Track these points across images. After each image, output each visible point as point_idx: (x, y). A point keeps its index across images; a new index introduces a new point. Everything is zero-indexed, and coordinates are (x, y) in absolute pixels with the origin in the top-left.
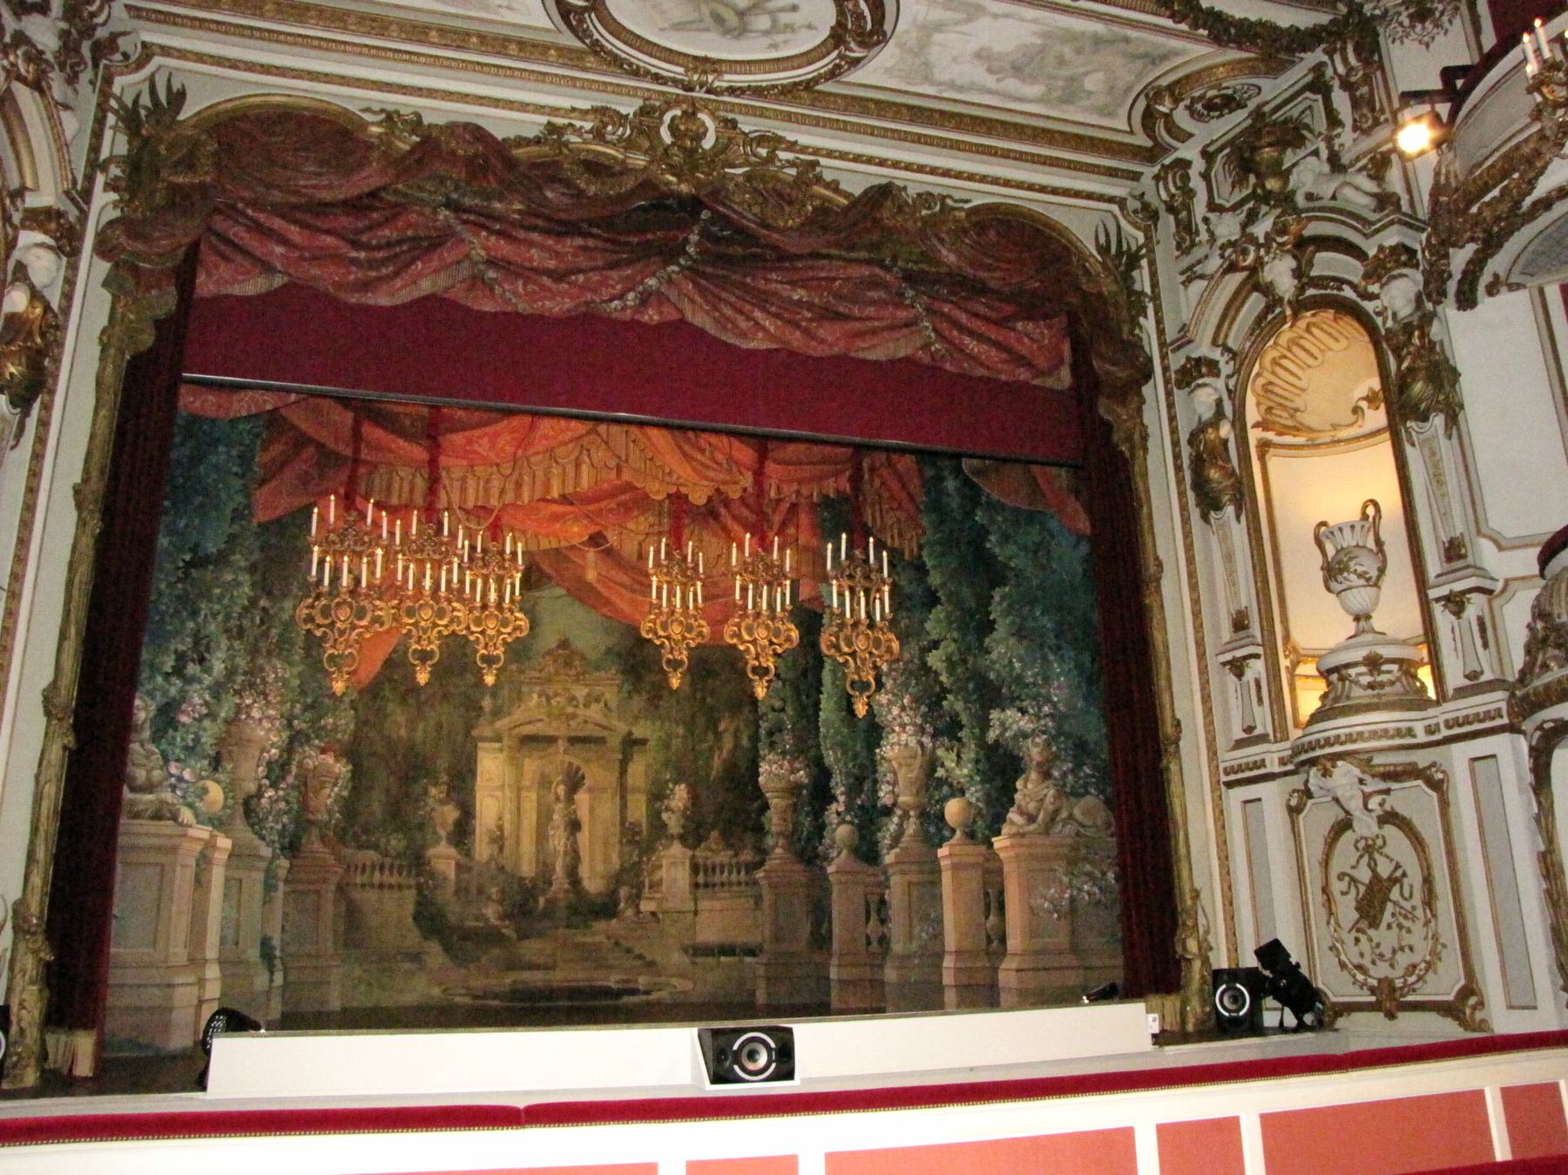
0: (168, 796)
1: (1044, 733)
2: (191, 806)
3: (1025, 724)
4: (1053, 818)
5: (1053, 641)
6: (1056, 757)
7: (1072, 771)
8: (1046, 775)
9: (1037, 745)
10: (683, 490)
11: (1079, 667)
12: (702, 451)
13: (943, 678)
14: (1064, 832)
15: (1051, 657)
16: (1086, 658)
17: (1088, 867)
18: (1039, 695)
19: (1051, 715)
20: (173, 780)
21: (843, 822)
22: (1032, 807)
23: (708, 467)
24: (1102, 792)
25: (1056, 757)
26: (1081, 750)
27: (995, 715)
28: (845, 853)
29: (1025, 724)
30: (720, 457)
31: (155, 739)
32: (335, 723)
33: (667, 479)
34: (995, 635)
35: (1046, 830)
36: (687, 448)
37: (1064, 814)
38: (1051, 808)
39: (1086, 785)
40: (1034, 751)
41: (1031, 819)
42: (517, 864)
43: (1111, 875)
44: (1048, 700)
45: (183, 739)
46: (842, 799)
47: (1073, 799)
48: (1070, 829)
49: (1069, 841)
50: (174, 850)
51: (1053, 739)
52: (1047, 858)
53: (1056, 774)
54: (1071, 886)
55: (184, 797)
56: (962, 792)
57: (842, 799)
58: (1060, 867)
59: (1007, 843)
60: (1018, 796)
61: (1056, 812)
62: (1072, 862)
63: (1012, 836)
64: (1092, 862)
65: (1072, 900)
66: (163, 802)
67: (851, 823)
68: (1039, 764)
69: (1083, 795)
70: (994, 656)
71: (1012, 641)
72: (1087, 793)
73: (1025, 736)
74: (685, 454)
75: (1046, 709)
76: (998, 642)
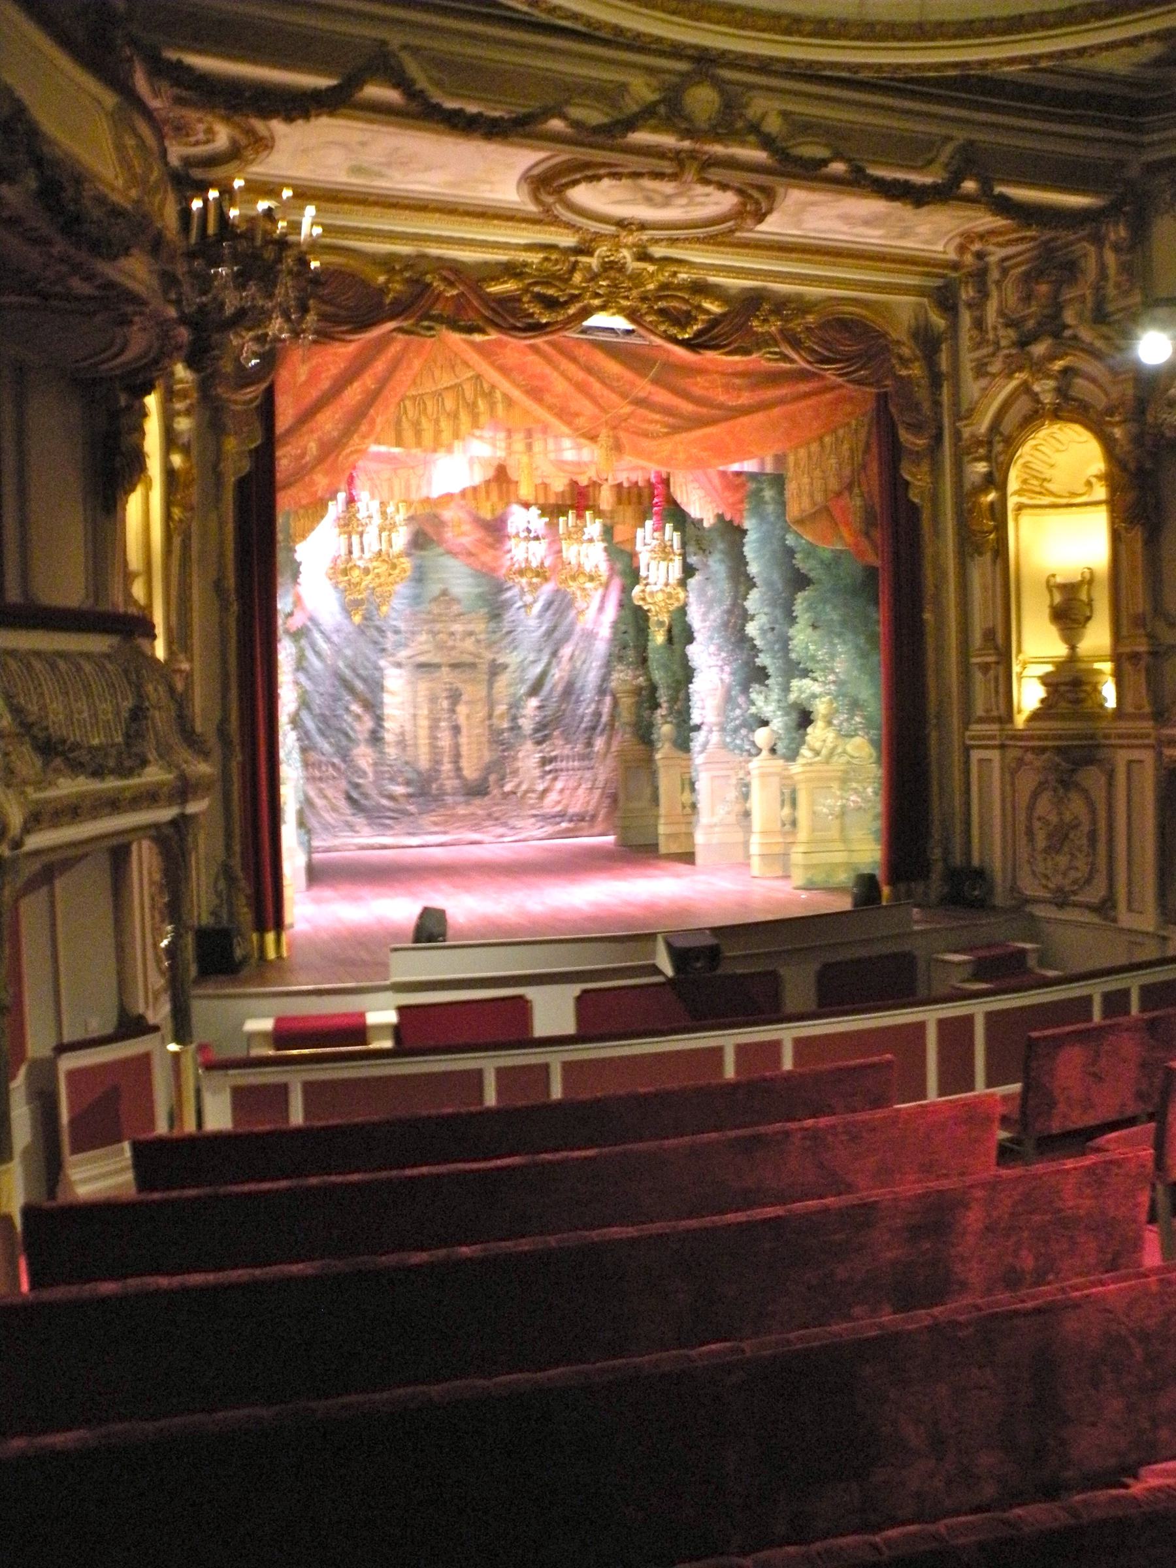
1: (828, 694)
3: (816, 688)
4: (832, 753)
5: (838, 630)
6: (837, 711)
7: (847, 720)
8: (829, 723)
9: (823, 703)
11: (857, 647)
13: (757, 642)
14: (839, 762)
15: (836, 641)
16: (862, 641)
17: (854, 785)
18: (826, 668)
19: (834, 682)
21: (667, 722)
22: (817, 745)
24: (867, 734)
25: (837, 711)
26: (855, 705)
27: (795, 683)
28: (667, 745)
29: (816, 688)
34: (798, 627)
35: (827, 761)
37: (839, 750)
38: (831, 745)
39: (856, 730)
40: (821, 708)
41: (817, 753)
42: (417, 756)
43: (870, 790)
44: (832, 671)
46: (665, 705)
47: (847, 740)
48: (845, 759)
49: (842, 768)
51: (836, 698)
52: (830, 779)
53: (835, 722)
54: (842, 798)
56: (765, 723)
57: (665, 705)
58: (835, 785)
59: (800, 769)
60: (808, 738)
61: (834, 748)
62: (844, 781)
63: (804, 765)
64: (858, 782)
65: (843, 807)
67: (671, 722)
68: (825, 716)
69: (852, 736)
70: (795, 642)
71: (810, 630)
72: (857, 735)
73: (814, 696)
75: (831, 678)
76: (800, 631)
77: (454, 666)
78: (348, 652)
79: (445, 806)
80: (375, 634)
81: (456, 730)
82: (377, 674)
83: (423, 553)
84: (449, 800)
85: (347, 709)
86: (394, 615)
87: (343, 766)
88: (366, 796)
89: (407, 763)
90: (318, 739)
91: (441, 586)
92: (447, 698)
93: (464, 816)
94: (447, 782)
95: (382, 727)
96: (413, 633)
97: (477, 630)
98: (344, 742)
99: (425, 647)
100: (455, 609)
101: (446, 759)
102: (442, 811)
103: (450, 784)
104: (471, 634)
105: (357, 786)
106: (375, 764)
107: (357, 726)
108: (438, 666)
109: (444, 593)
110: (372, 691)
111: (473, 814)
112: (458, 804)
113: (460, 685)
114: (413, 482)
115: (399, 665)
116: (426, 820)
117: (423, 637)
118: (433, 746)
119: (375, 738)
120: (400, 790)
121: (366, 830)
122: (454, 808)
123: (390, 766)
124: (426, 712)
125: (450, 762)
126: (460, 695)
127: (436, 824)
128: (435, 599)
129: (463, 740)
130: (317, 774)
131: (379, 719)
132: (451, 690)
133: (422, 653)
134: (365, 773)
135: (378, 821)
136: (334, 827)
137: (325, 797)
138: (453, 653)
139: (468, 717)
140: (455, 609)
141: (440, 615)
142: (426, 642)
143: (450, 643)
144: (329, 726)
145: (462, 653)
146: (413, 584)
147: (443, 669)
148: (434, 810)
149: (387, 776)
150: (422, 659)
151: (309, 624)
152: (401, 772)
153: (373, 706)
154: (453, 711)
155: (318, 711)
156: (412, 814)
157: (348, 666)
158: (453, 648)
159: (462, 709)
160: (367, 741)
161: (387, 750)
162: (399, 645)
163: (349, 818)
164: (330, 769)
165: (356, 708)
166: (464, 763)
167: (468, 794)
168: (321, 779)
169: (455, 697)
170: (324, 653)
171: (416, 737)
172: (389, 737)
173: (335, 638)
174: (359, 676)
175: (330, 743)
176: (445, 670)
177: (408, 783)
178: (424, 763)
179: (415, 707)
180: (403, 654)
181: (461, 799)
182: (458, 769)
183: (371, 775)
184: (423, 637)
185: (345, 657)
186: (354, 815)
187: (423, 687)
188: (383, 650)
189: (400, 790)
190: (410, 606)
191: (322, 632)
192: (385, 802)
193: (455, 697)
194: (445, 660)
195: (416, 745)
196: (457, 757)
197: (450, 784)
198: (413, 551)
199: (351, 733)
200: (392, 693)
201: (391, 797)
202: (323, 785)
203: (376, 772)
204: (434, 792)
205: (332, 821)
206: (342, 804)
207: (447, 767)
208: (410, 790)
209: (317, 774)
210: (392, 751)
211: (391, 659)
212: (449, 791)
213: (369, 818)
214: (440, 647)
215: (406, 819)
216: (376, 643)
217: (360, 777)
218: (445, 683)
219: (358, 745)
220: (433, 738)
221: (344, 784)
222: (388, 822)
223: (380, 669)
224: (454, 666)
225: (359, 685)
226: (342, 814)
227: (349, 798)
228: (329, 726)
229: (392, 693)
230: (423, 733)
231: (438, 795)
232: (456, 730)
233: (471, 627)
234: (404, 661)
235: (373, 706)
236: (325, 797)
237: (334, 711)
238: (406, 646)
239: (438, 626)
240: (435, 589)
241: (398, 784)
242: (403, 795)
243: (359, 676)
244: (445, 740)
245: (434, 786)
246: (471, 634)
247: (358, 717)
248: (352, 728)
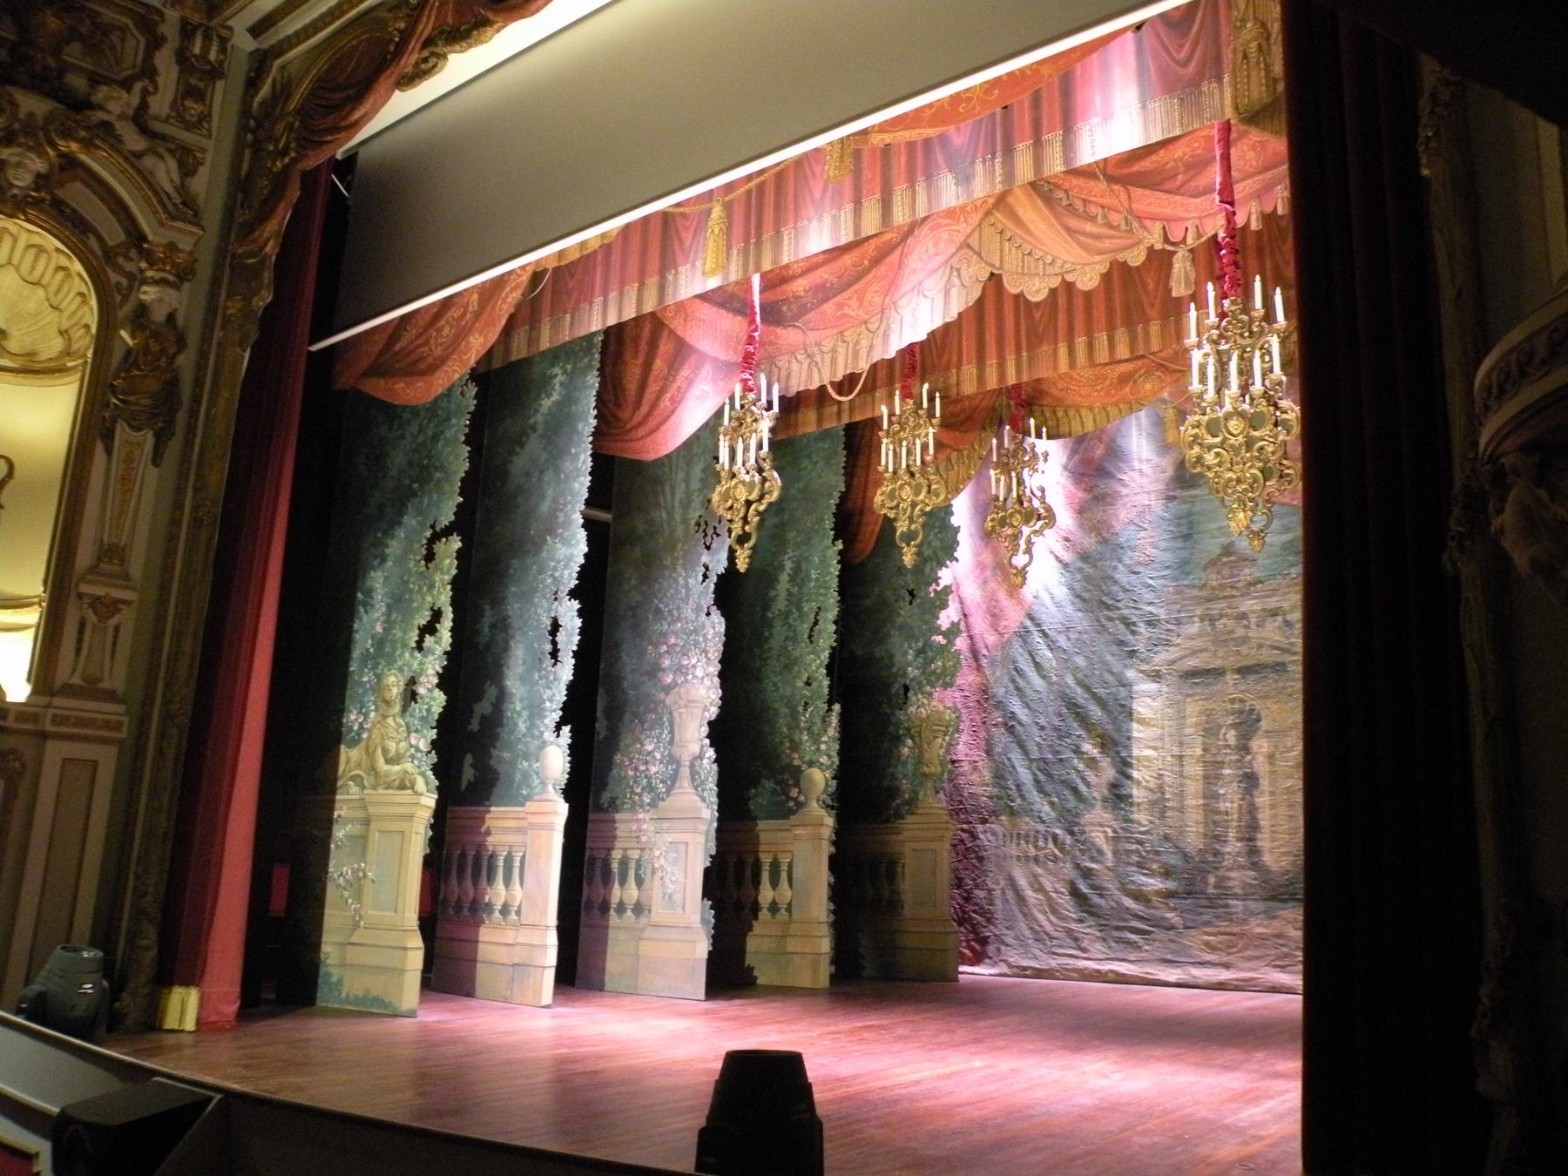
0: (408, 766)
2: (423, 774)
10: (1069, 278)
12: (1092, 219)
20: (412, 750)
23: (1097, 237)
30: (1116, 218)
31: (404, 709)
32: (944, 665)
33: (1050, 270)
36: (1074, 223)
45: (420, 710)
50: (411, 817)
55: (419, 767)
66: (406, 772)
74: (1069, 230)
77: (1243, 671)
78: (1080, 661)
79: (1229, 917)
80: (1121, 626)
81: (1250, 781)
82: (1123, 692)
83: (1193, 492)
84: (1237, 905)
85: (1078, 751)
86: (1149, 596)
87: (1069, 840)
88: (1100, 890)
89: (1166, 838)
90: (1035, 796)
91: (1224, 540)
92: (1234, 726)
93: (1263, 937)
94: (1233, 874)
95: (1129, 777)
96: (1178, 622)
97: (1286, 605)
98: (1072, 802)
99: (1198, 643)
100: (1247, 573)
101: (1232, 834)
102: (1223, 925)
103: (1238, 878)
104: (1274, 613)
105: (1087, 874)
106: (1116, 839)
107: (1092, 778)
108: (1218, 673)
109: (1228, 550)
110: (1114, 721)
111: (1279, 936)
112: (1252, 914)
113: (1258, 705)
114: (864, 343)
115: (1156, 676)
116: (1194, 939)
117: (1194, 628)
118: (1209, 810)
119: (1118, 797)
120: (1154, 884)
121: (1098, 948)
122: (1245, 922)
123: (1140, 842)
124: (1199, 752)
125: (1240, 840)
126: (1258, 720)
127: (1212, 948)
128: (1213, 563)
129: (1262, 800)
130: (1032, 851)
131: (1124, 765)
132: (1241, 712)
133: (1194, 653)
134: (1100, 852)
135: (1116, 934)
136: (1051, 938)
137: (1040, 889)
138: (1244, 650)
139: (1271, 757)
140: (1247, 573)
141: (1222, 587)
142: (1200, 635)
143: (1240, 632)
144: (1049, 775)
145: (1260, 646)
146: (1179, 544)
147: (1229, 676)
148: (1208, 923)
149: (1135, 858)
150: (1193, 663)
151: (1028, 623)
152: (1157, 853)
153: (1115, 743)
154: (1245, 749)
155: (1035, 755)
156: (1172, 928)
157: (1079, 683)
158: (1245, 640)
159: (1260, 745)
160: (1105, 800)
161: (1135, 816)
162: (1155, 644)
163: (1073, 926)
164: (1051, 845)
165: (1088, 747)
166: (1264, 841)
167: (1273, 898)
168: (1036, 860)
169: (1248, 724)
170: (1046, 665)
171: (1181, 795)
172: (1138, 794)
173: (1062, 642)
174: (1095, 696)
175: (1052, 804)
176: (1230, 678)
177: (1167, 873)
178: (1194, 840)
179: (1181, 744)
180: (1162, 657)
181: (1260, 906)
182: (1253, 851)
183: (1110, 856)
184: (1194, 628)
185: (1076, 670)
186: (1081, 921)
187: (1193, 709)
188: (1132, 653)
189: (1154, 884)
190: (1175, 579)
191: (1045, 635)
192: (1128, 902)
193: (1248, 724)
194: (1233, 662)
195: (1181, 809)
196: (1250, 830)
197: (1238, 878)
198: (1177, 493)
199: (1082, 788)
200: (1142, 722)
201: (1139, 896)
202: (1039, 871)
203: (1115, 853)
204: (1211, 890)
205: (1049, 928)
206: (1065, 901)
207: (1233, 846)
208: (1171, 885)
209: (1032, 851)
210: (1141, 817)
211: (1144, 667)
212: (1238, 891)
213: (1102, 927)
214: (1221, 640)
215: (1160, 934)
216: (1121, 643)
217: (1093, 859)
218: (1232, 701)
219: (1092, 806)
220: (1210, 796)
221: (1068, 870)
222: (1134, 937)
223: (1126, 685)
224: (1243, 671)
225: (1095, 712)
226: (1063, 918)
227: (1075, 892)
228: (1049, 775)
229: (1142, 722)
230: (1194, 788)
231: (1219, 897)
232: (1250, 781)
233: (1272, 603)
234: (1164, 670)
235: (1114, 745)
236: (1040, 889)
237: (1058, 752)
238: (1168, 643)
239: (1216, 608)
240: (1212, 546)
241: (1152, 874)
242: (1158, 893)
243: (1095, 696)
244: (1230, 799)
245: (1212, 879)
246: (1274, 613)
247: (1092, 763)
248: (1084, 779)
